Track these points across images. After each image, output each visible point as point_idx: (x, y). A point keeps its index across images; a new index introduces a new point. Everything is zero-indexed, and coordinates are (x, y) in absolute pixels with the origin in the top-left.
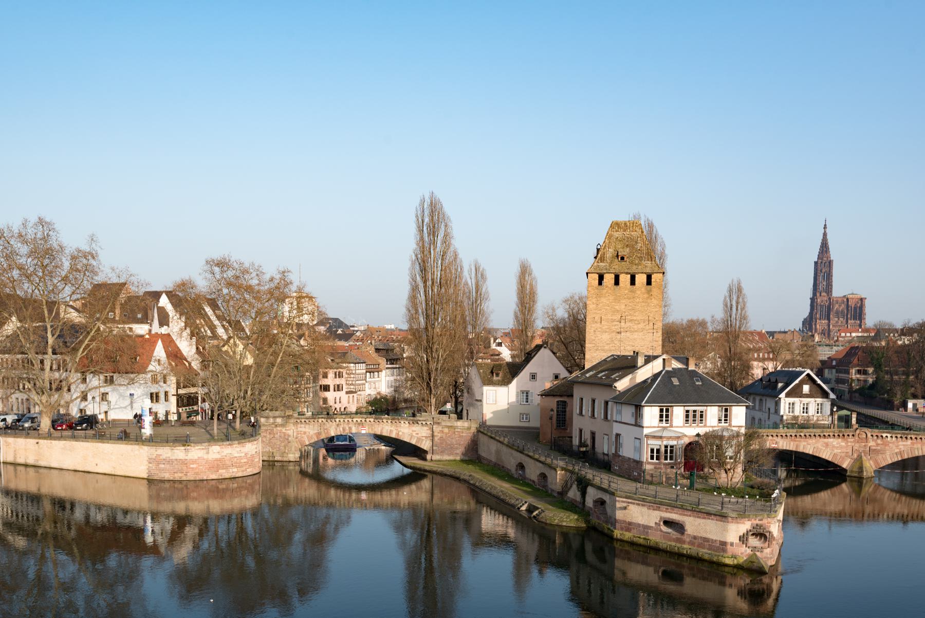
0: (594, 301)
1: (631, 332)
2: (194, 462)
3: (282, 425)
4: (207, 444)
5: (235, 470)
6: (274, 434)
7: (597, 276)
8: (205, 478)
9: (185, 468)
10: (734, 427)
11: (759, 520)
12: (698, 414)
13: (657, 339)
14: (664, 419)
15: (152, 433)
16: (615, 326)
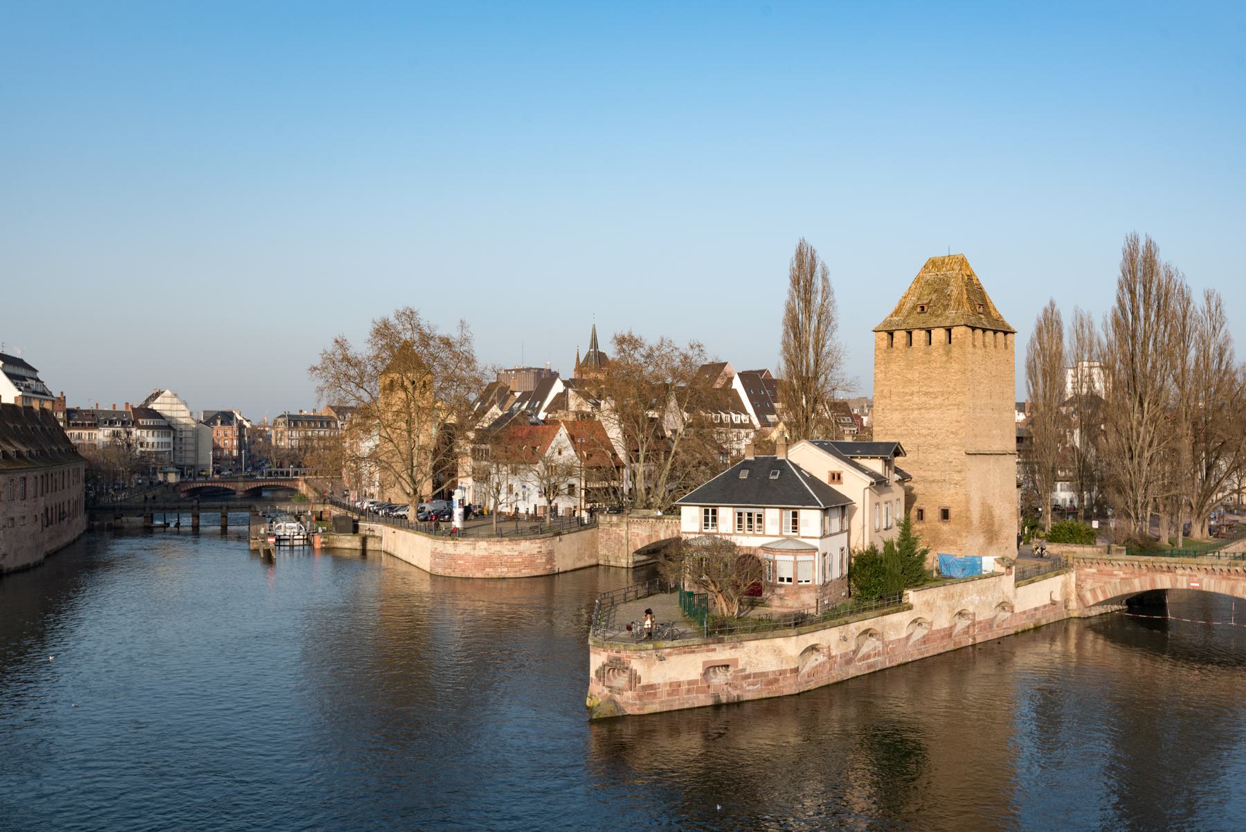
0: (882, 368)
1: (926, 409)
2: (461, 557)
3: (617, 525)
4: (473, 539)
5: (506, 570)
6: (610, 535)
7: (885, 335)
8: (471, 576)
9: (453, 564)
10: (803, 537)
11: (617, 652)
12: (755, 518)
13: (959, 419)
14: (710, 523)
15: (190, 515)
16: (907, 401)
